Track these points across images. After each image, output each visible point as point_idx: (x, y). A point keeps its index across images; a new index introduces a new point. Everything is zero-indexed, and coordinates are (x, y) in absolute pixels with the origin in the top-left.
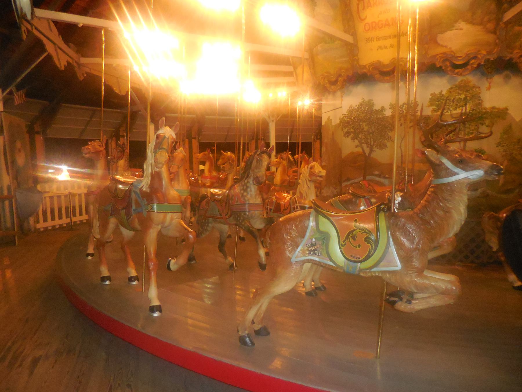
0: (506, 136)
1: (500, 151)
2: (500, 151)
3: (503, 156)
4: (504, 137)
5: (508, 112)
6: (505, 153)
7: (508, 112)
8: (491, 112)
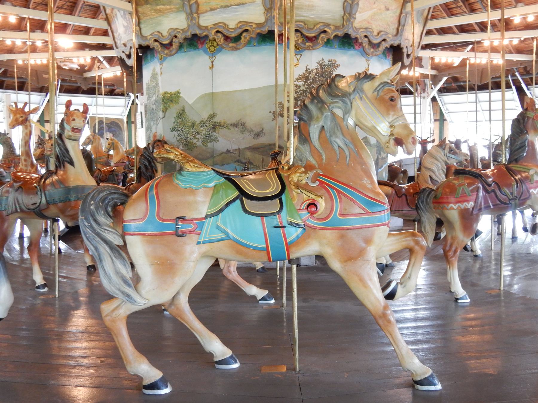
0: (180, 120)
1: (175, 136)
2: (175, 136)
3: (178, 141)
4: (178, 121)
5: (180, 95)
6: (179, 137)
7: (180, 95)
8: (164, 97)
